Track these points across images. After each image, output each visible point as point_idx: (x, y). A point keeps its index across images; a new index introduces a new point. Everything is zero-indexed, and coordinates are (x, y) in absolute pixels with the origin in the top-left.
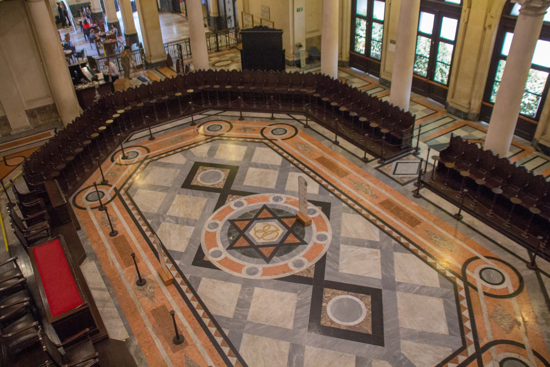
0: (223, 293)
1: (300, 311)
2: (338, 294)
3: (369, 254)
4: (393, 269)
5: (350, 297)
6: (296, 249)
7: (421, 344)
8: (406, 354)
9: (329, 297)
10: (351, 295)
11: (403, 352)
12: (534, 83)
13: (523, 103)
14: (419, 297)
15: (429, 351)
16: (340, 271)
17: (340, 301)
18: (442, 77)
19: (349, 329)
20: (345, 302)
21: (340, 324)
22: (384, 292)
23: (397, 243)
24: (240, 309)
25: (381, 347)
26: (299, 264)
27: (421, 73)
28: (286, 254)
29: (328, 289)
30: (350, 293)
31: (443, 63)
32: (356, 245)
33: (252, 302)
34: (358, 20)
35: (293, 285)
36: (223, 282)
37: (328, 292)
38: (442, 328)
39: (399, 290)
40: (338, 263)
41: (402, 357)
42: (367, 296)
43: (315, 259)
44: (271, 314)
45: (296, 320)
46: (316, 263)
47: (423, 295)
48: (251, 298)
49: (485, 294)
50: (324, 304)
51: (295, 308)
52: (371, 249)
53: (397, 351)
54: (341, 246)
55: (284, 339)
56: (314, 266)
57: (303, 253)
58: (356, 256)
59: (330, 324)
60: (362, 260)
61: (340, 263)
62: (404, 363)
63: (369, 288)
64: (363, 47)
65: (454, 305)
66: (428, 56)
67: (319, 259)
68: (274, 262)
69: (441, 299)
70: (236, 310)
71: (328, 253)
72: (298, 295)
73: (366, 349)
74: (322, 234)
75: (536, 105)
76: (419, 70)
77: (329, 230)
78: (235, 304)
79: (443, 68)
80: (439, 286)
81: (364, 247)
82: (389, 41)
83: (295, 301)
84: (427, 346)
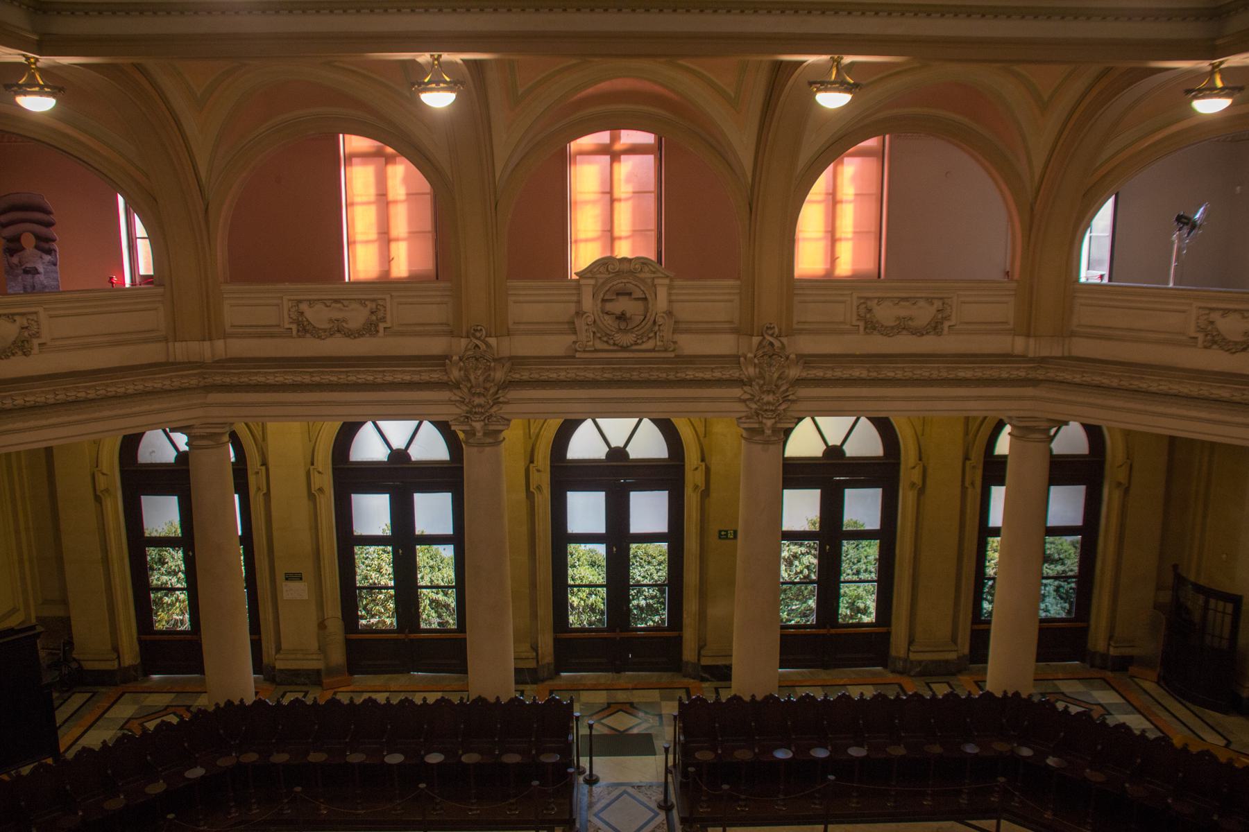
12: (647, 567)
13: (638, 607)
18: (440, 616)
27: (380, 625)
31: (438, 587)
34: (152, 553)
64: (183, 614)
66: (392, 583)
75: (663, 603)
76: (374, 621)
79: (440, 597)
82: (280, 577)
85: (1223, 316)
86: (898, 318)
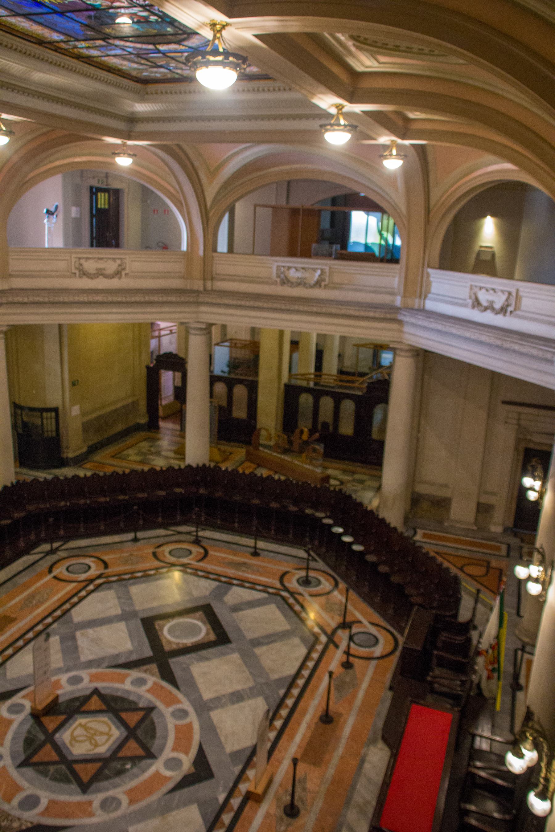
36: (218, 731)
85: (86, 261)
86: (97, 269)
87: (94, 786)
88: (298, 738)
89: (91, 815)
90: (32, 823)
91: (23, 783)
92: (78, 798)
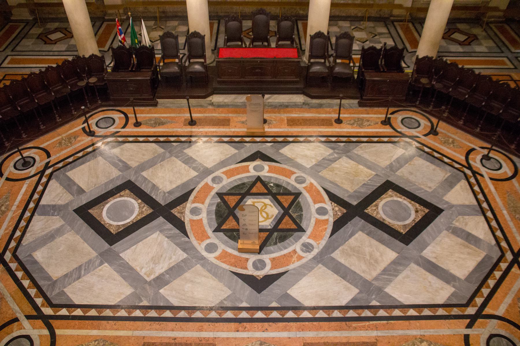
0: (211, 155)
1: (150, 185)
2: (138, 215)
3: (153, 268)
4: (117, 272)
5: (128, 221)
6: (215, 220)
7: (48, 231)
8: (55, 217)
9: (143, 208)
10: (129, 222)
11: (58, 217)
14: (75, 266)
15: (39, 231)
16: (158, 232)
17: (132, 212)
19: (106, 201)
20: (127, 214)
21: (116, 199)
22: (106, 246)
23: (141, 304)
24: (187, 157)
25: (75, 208)
26: (195, 211)
28: (216, 210)
29: (150, 212)
30: (131, 223)
32: (173, 267)
33: (186, 166)
35: (178, 195)
36: (222, 160)
37: (147, 210)
38: (39, 255)
39: (97, 257)
40: (168, 237)
41: (56, 214)
42: (116, 232)
43: (189, 225)
44: (165, 170)
45: (146, 179)
46: (184, 223)
47: (73, 270)
48: (190, 167)
49: (16, 320)
50: (140, 201)
51: (155, 183)
52: (157, 275)
53: (62, 215)
54: (185, 255)
55: (138, 167)
56: (183, 219)
57: (205, 221)
58: (162, 256)
59: (122, 194)
60: (153, 257)
61: (166, 239)
62: (52, 211)
63: (122, 239)
65: (41, 283)
67: (187, 228)
68: (213, 197)
69: (55, 279)
70: (188, 155)
71: (187, 239)
72: (164, 193)
73: (84, 200)
74: (215, 251)
77: (216, 260)
78: (193, 157)
80: (65, 290)
81: (165, 272)
83: (161, 187)
84: (43, 233)
87: (293, 191)
88: (214, 130)
89: (311, 184)
90: (331, 203)
91: (313, 221)
92: (305, 194)
